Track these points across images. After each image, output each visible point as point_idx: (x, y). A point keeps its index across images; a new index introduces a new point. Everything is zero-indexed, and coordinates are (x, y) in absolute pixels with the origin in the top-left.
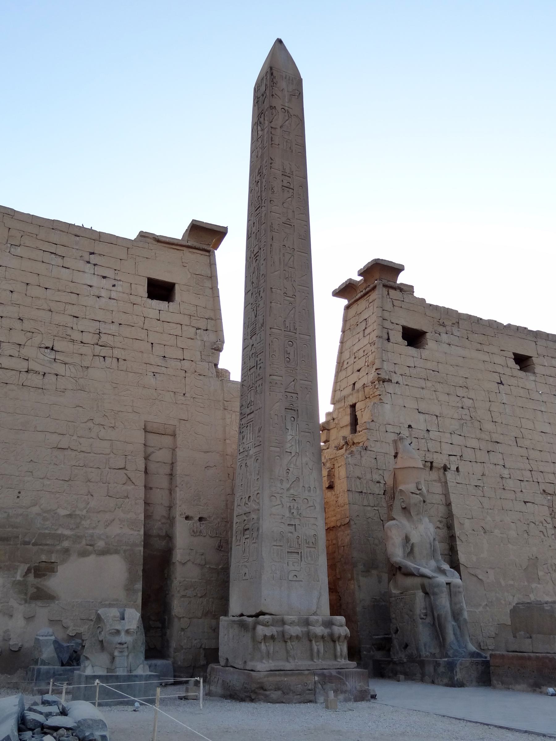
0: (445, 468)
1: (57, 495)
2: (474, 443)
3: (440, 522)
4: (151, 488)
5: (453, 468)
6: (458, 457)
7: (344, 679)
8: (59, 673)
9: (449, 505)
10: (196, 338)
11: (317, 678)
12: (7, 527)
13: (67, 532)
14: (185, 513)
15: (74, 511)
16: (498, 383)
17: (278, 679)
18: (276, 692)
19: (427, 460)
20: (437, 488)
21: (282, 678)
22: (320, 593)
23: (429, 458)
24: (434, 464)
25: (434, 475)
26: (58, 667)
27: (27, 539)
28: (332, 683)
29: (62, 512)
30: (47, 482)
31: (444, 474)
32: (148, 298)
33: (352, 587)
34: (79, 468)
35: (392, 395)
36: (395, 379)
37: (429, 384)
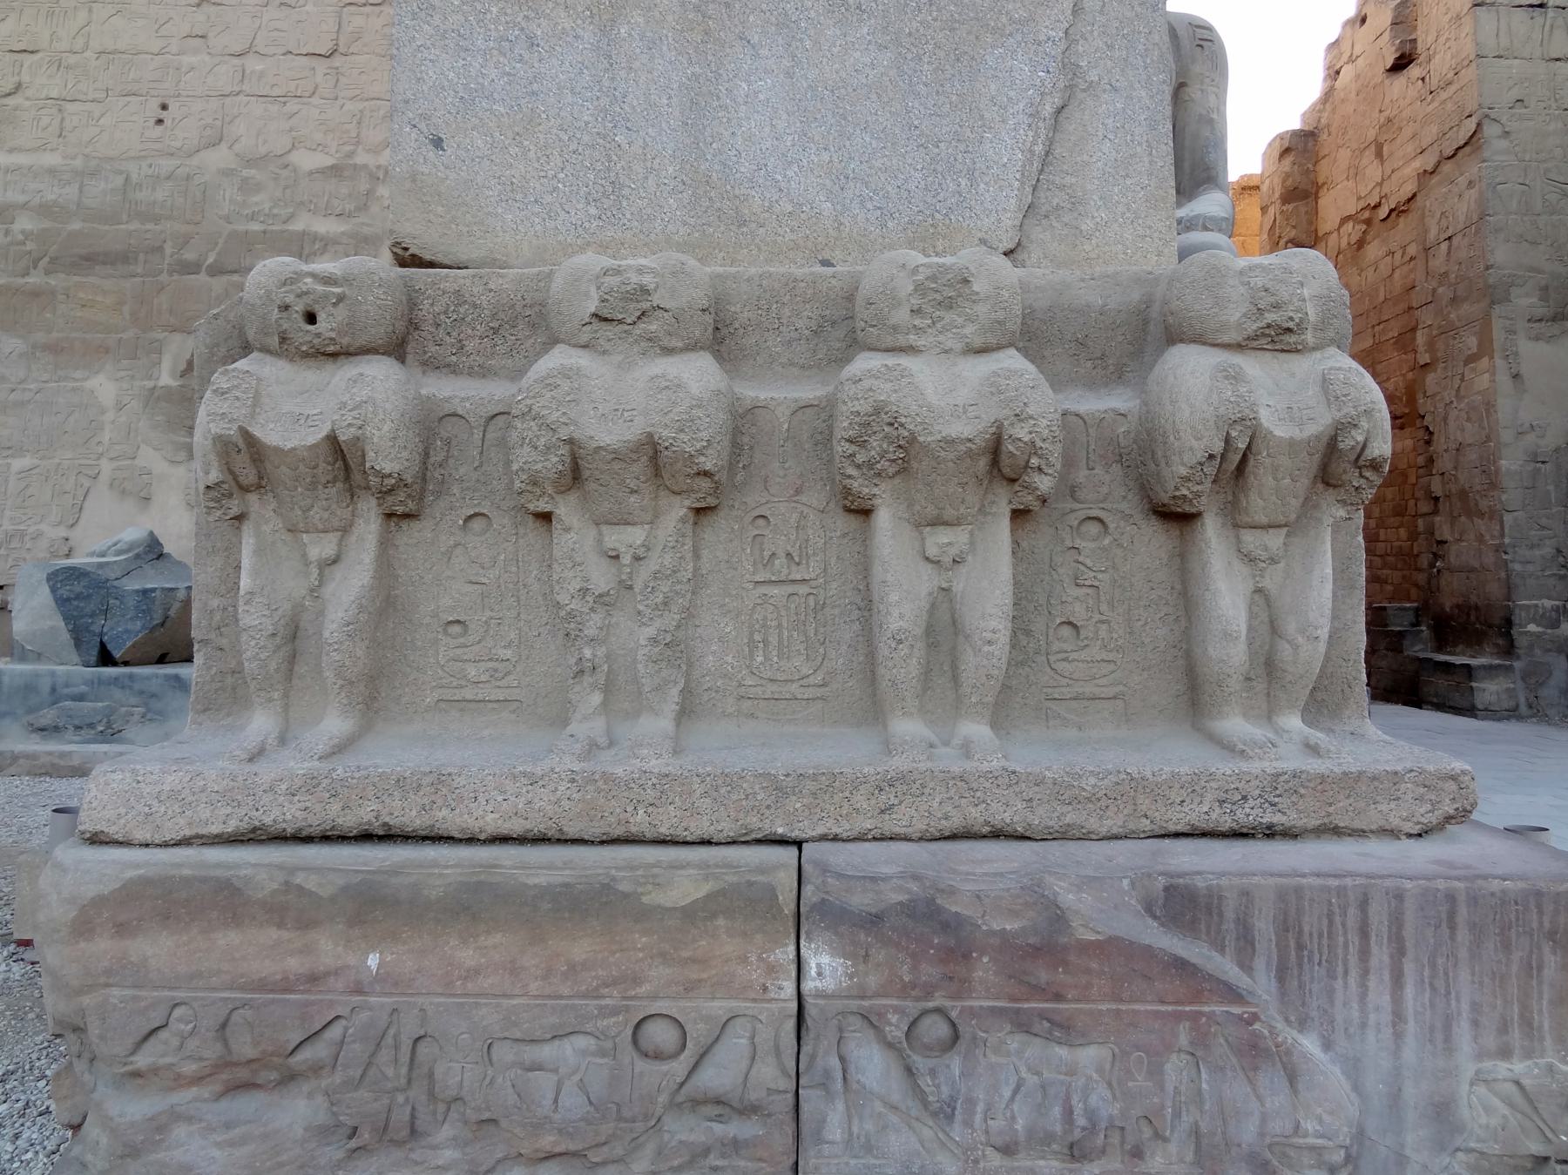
1: (292, 106)
7: (1261, 984)
8: (75, 690)
11: (825, 966)
12: (125, 217)
13: (325, 226)
15: (351, 155)
17: (255, 951)
18: (246, 1104)
21: (328, 949)
22: (1070, 68)
26: (74, 670)
27: (189, 255)
28: (1065, 1030)
29: (307, 161)
30: (254, 65)
33: (1483, 381)
34: (368, 9)
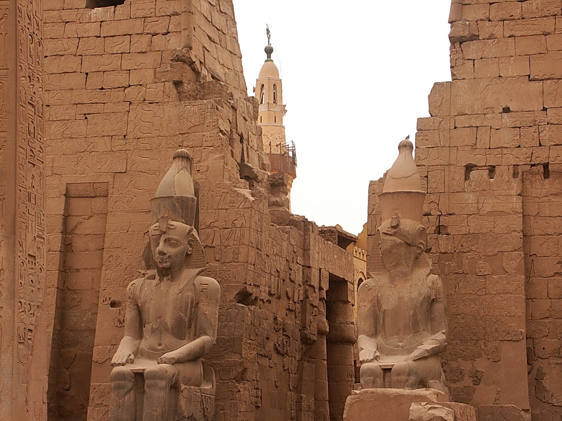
4: (78, 270)
14: (110, 298)
23: (541, 156)
32: (87, 7)
36: (486, 29)
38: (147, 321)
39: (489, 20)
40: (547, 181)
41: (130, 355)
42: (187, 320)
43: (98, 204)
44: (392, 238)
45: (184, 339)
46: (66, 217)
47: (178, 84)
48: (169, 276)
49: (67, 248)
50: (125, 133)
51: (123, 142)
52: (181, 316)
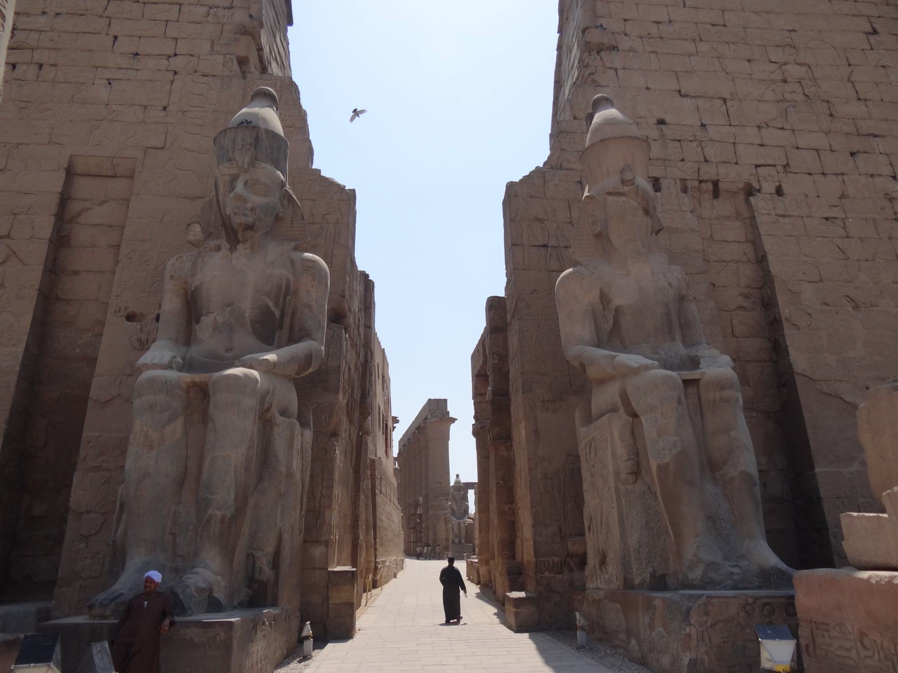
0: (750, 191)
2: (819, 140)
3: (746, 296)
4: (76, 273)
5: (768, 187)
6: (781, 169)
9: (761, 260)
10: (207, 22)
14: (126, 308)
16: (867, 33)
19: (704, 177)
20: (735, 231)
23: (709, 172)
24: (722, 186)
25: (724, 207)
31: (748, 202)
35: (620, 72)
37: (704, 47)
38: (205, 312)
39: (626, 35)
40: (715, 202)
41: (174, 357)
42: (277, 313)
43: (117, 186)
44: (624, 198)
45: (271, 344)
46: (65, 199)
47: (242, 62)
48: (248, 244)
49: (60, 240)
50: (165, 104)
51: (163, 113)
52: (267, 307)
